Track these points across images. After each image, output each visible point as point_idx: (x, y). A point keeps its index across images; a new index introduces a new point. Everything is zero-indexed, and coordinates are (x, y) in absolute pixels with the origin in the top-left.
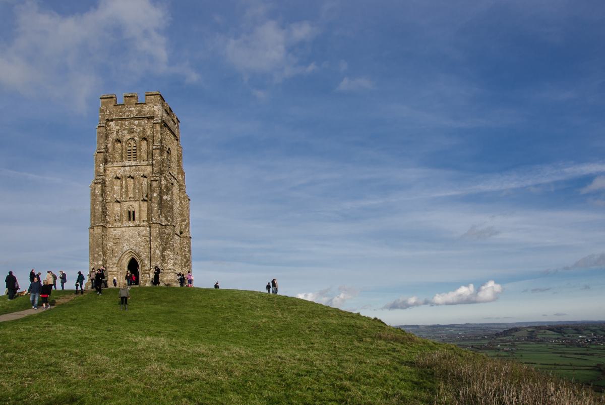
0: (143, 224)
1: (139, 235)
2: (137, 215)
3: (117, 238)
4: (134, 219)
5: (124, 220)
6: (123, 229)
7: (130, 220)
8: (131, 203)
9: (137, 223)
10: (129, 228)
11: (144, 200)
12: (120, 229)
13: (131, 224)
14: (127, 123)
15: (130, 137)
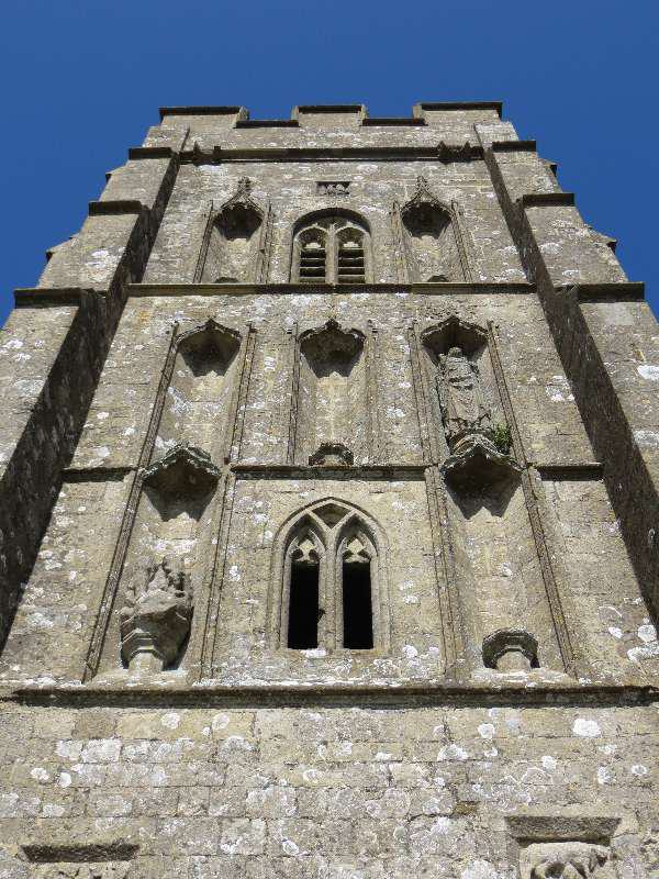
0: (482, 676)
1: (465, 809)
2: (401, 590)
3: (101, 831)
4: (359, 633)
5: (236, 625)
6: (222, 718)
7: (302, 632)
8: (331, 490)
9: (410, 658)
10: (314, 715)
11: (479, 479)
12: (172, 717)
13: (328, 665)
14: (306, 167)
15: (322, 205)
